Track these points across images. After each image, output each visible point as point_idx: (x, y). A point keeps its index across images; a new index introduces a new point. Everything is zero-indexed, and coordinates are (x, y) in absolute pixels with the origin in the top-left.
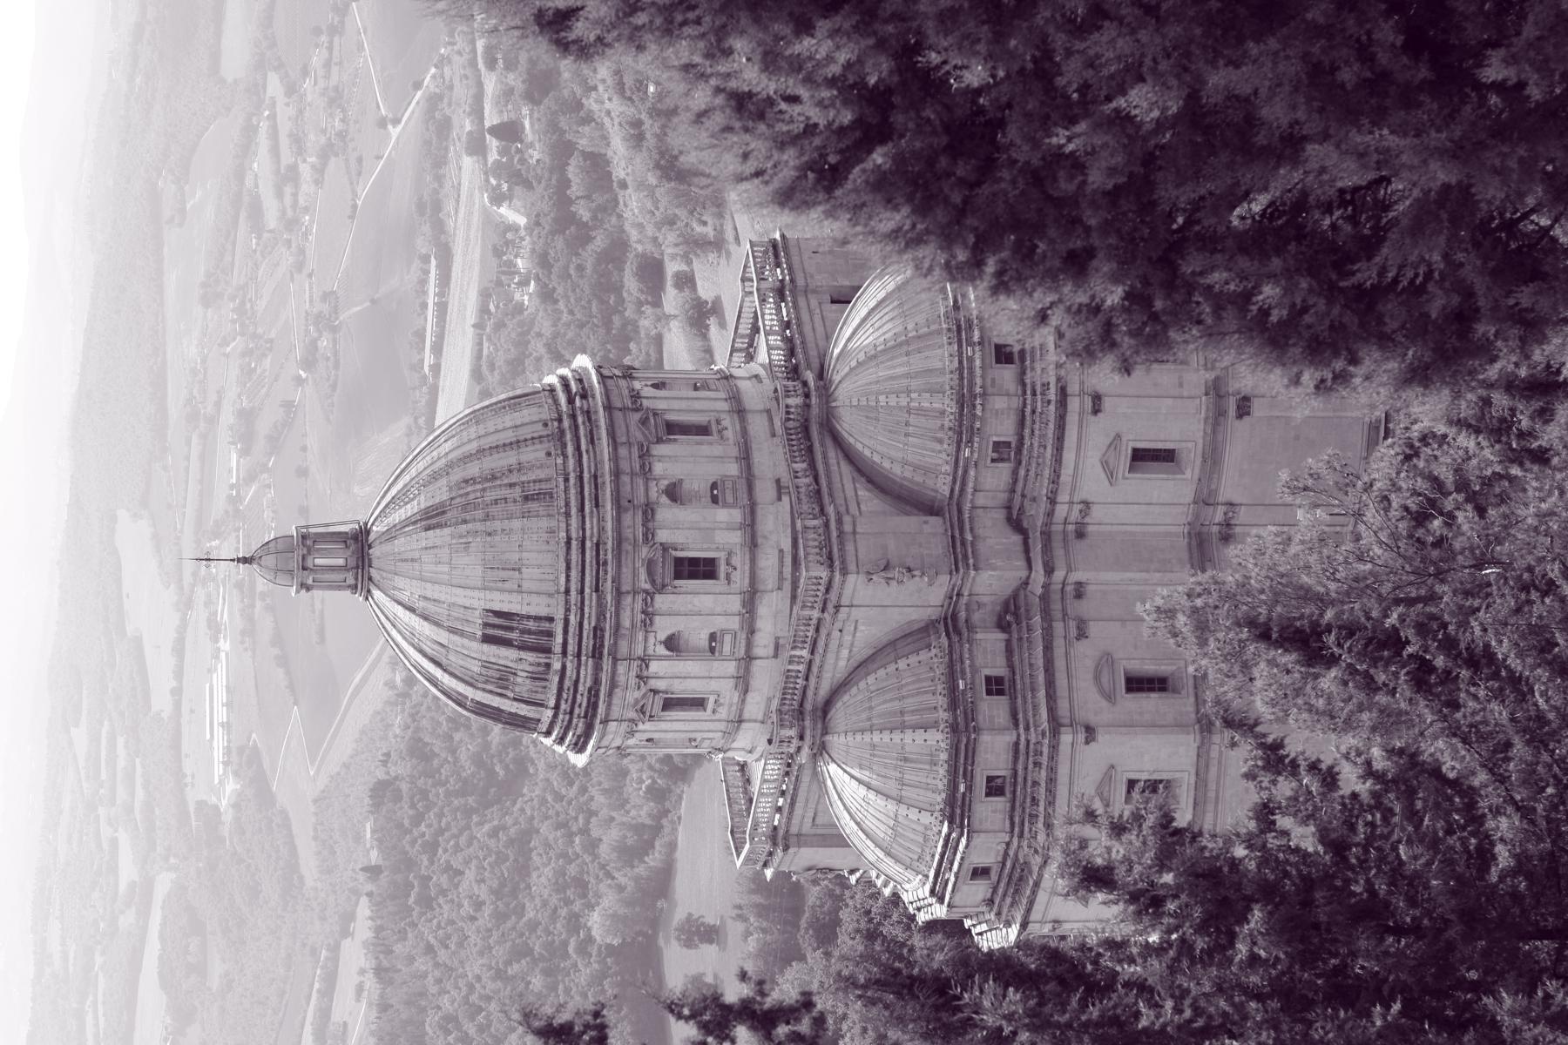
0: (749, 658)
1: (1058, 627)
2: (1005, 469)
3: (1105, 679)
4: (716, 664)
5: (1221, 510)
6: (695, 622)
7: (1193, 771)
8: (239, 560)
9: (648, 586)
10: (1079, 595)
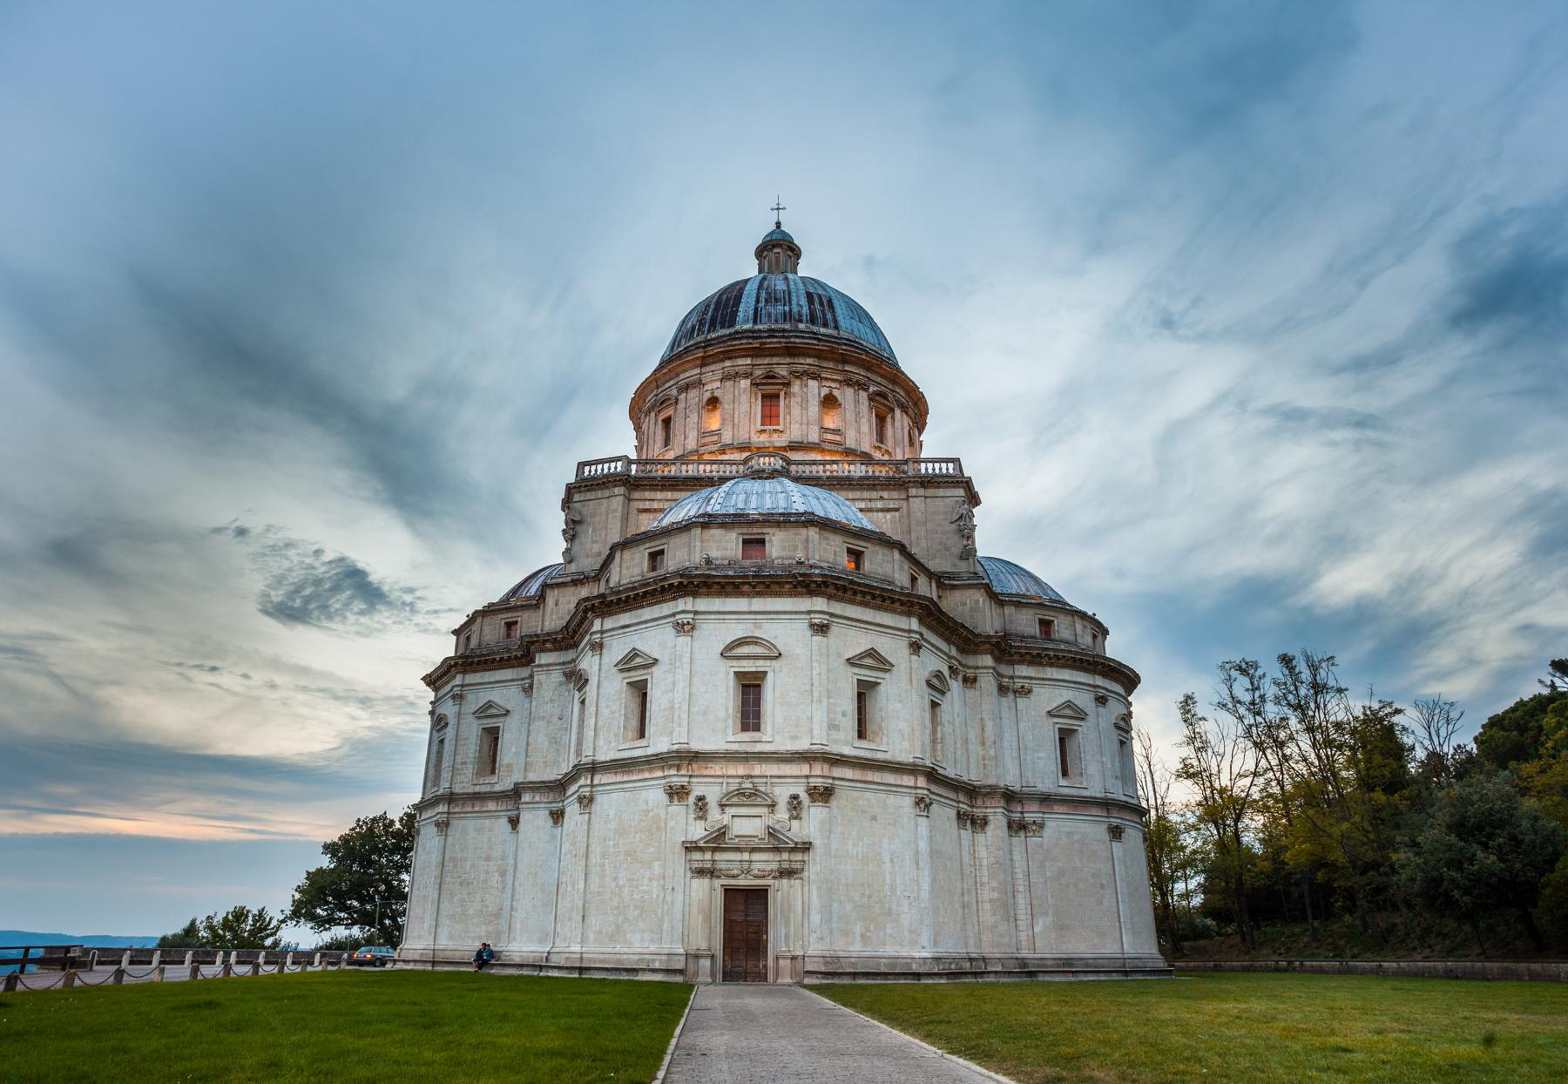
0: (823, 451)
1: (954, 652)
2: (1035, 630)
3: (935, 681)
4: (816, 428)
5: (1037, 816)
6: (850, 416)
7: (888, 757)
8: (778, 225)
9: (872, 389)
10: (965, 680)
